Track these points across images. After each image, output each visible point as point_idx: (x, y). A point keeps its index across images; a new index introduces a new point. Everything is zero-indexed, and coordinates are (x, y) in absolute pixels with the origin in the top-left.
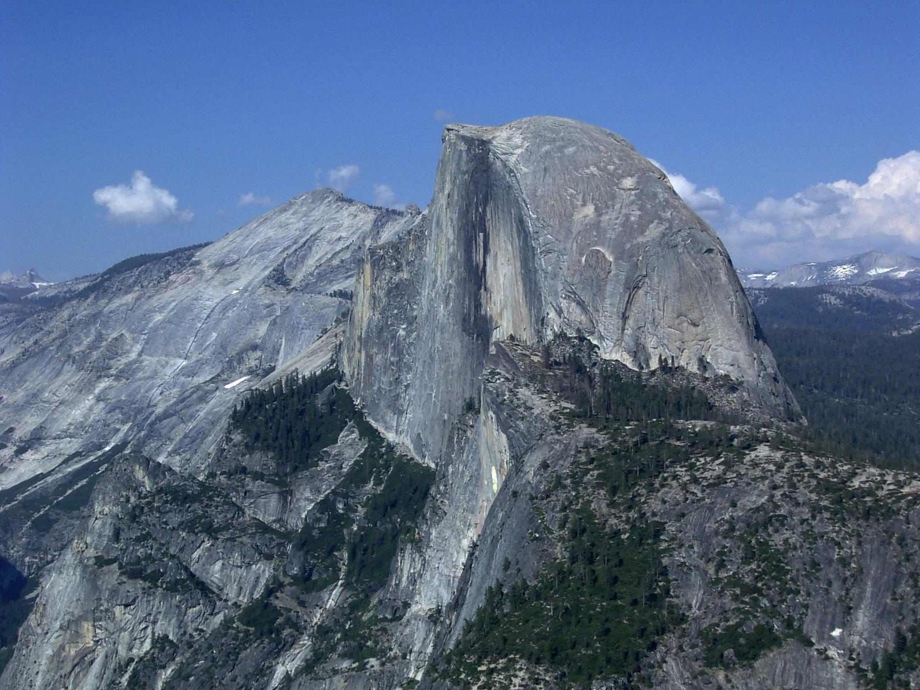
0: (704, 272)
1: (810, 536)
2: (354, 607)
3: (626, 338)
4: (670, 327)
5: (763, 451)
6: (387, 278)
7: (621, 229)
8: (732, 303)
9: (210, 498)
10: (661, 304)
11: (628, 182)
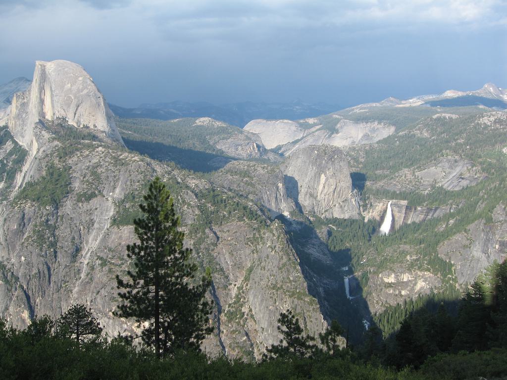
1: (107, 170)
2: (6, 188)
3: (75, 119)
5: (100, 148)
11: (81, 79)
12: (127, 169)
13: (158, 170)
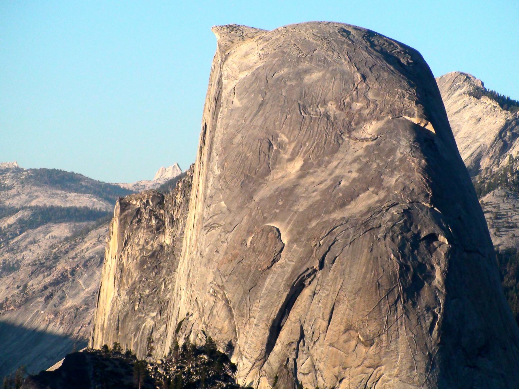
0: (404, 269)
4: (332, 345)
6: (142, 242)
7: (318, 198)
8: (435, 317)
10: (328, 311)
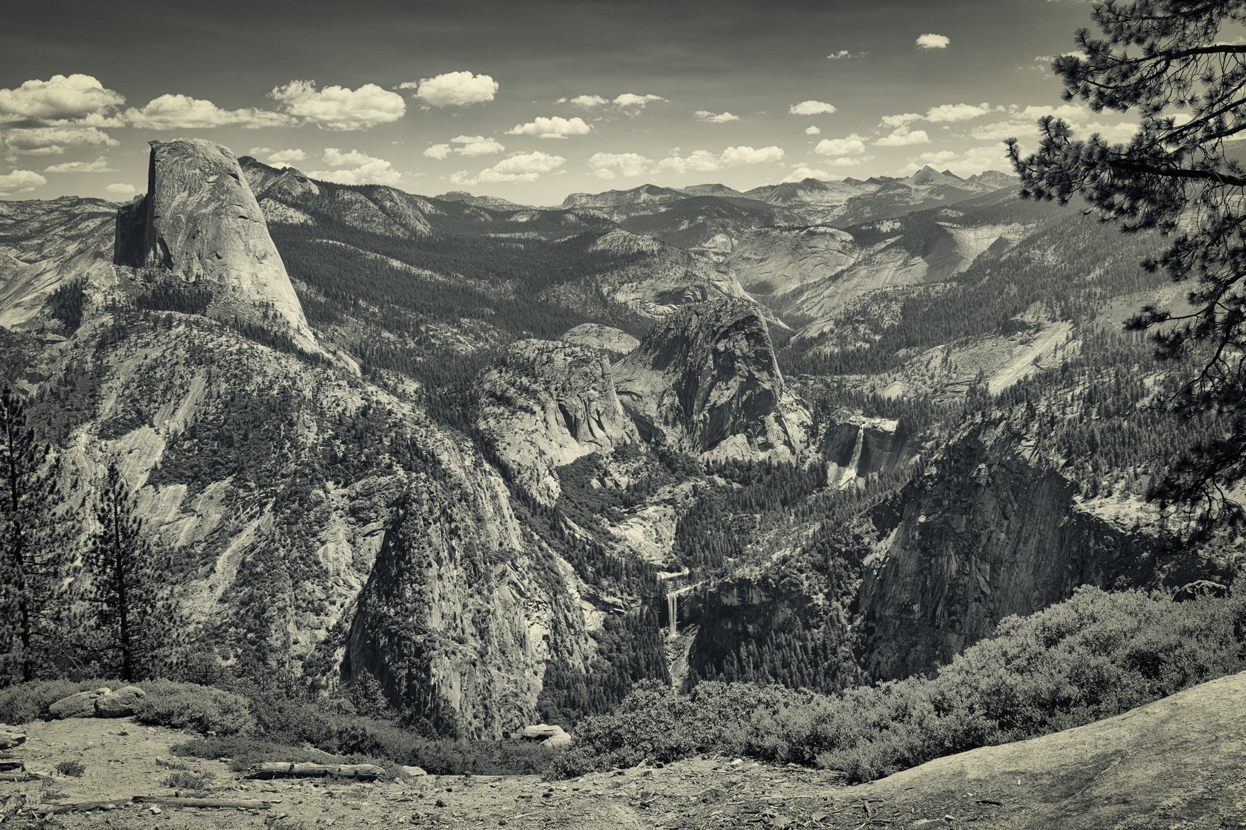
5: (181, 328)
9: (26, 344)
11: (212, 179)
12: (209, 373)
13: (270, 372)
